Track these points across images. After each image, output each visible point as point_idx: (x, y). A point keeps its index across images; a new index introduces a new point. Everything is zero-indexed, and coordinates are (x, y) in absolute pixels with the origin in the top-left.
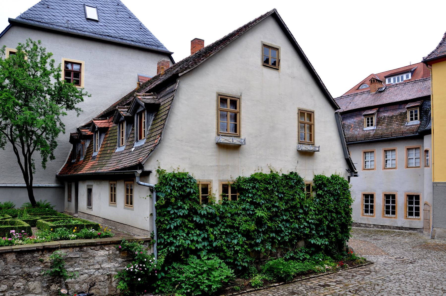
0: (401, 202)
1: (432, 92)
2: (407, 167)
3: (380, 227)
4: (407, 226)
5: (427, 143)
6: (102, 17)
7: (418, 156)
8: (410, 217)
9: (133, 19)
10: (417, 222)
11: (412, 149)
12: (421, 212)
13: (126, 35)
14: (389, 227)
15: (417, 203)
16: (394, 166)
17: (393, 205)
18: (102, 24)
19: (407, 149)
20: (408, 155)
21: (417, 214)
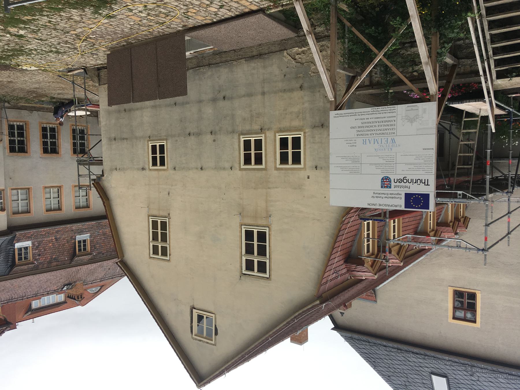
0: (35, 143)
4: (24, 113)
6: (426, 378)
9: (385, 374)
12: (6, 131)
13: (392, 354)
18: (426, 369)
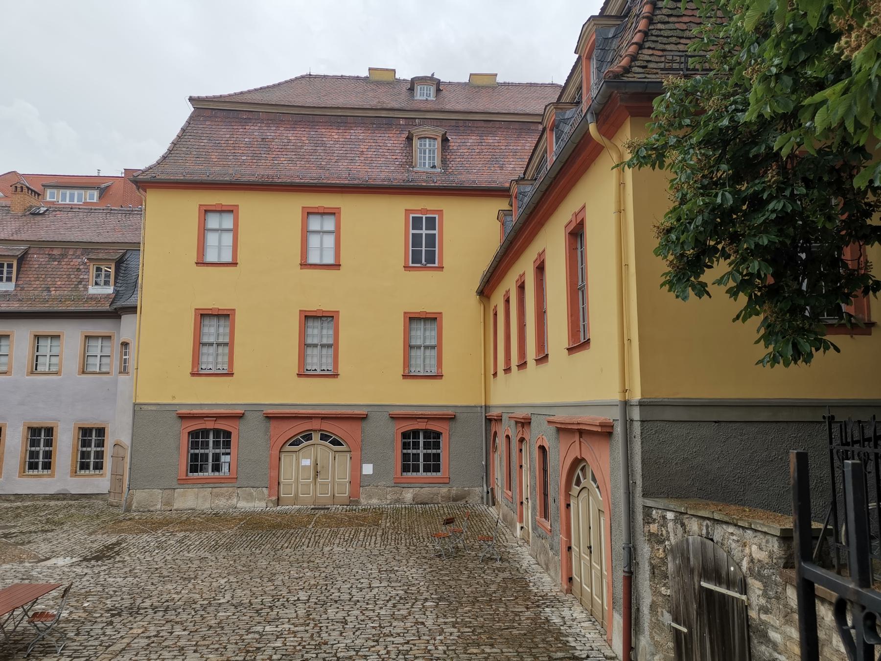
1: (144, 238)
2: (83, 372)
3: (12, 498)
5: (127, 327)
7: (107, 351)
8: (83, 472)
10: (98, 483)
11: (97, 337)
14: (33, 497)
15: (101, 444)
16: (54, 369)
17: (47, 449)
19: (86, 337)
20: (85, 349)
21: (99, 466)
